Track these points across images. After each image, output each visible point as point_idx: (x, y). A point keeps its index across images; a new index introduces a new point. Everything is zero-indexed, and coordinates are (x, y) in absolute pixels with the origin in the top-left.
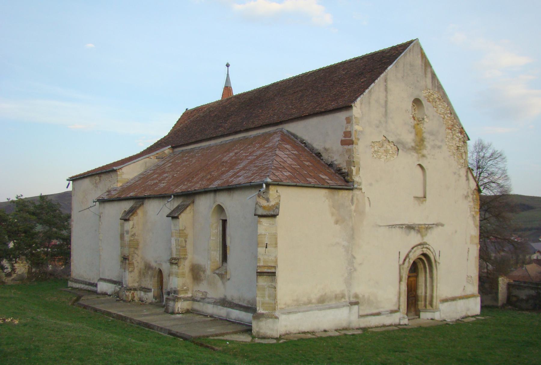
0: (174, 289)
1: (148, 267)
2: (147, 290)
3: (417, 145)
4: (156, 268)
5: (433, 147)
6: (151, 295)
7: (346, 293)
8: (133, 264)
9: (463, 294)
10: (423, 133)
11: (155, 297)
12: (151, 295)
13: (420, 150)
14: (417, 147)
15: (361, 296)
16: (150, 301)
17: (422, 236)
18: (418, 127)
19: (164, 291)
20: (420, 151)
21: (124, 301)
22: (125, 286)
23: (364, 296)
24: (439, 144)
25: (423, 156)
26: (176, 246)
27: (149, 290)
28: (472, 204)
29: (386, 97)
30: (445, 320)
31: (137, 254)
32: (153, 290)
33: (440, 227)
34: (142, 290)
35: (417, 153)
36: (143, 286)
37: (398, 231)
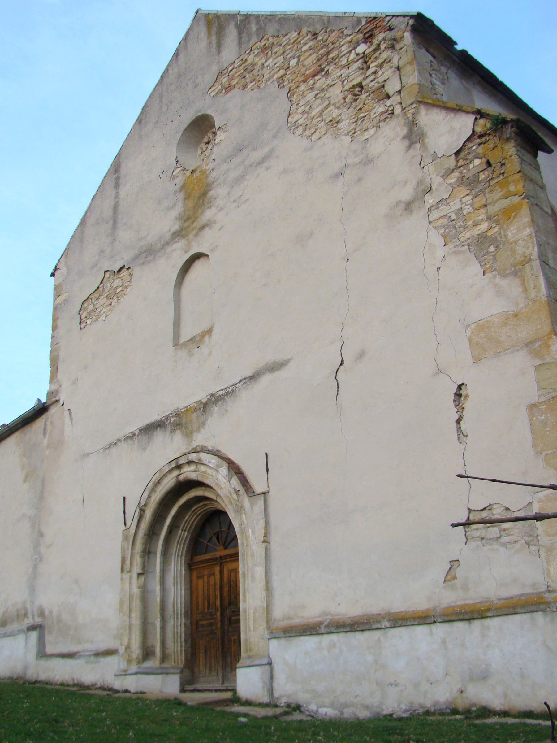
3: (188, 219)
5: (241, 178)
7: (29, 606)
9: (450, 598)
10: (207, 177)
13: (193, 222)
14: (186, 225)
15: (47, 612)
17: (189, 435)
18: (197, 174)
20: (195, 224)
23: (51, 612)
24: (266, 150)
25: (203, 227)
28: (463, 201)
29: (117, 196)
30: (298, 708)
33: (266, 379)
35: (184, 237)
37: (124, 446)
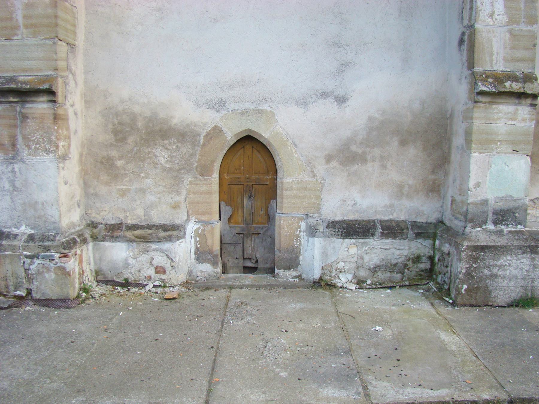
0: (493, 205)
1: (135, 136)
2: (150, 233)
4: (217, 131)
6: (184, 249)
8: (66, 119)
11: (201, 255)
12: (184, 249)
16: (182, 277)
19: (288, 223)
21: (46, 303)
22: (24, 230)
26: (512, 21)
27: (171, 231)
31: (74, 75)
32: (191, 227)
34: (114, 238)
36: (108, 214)
